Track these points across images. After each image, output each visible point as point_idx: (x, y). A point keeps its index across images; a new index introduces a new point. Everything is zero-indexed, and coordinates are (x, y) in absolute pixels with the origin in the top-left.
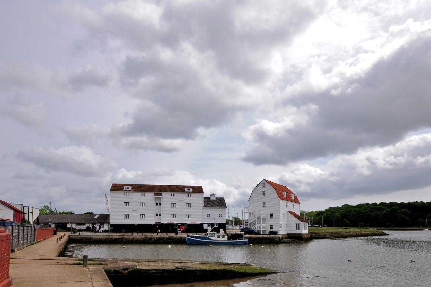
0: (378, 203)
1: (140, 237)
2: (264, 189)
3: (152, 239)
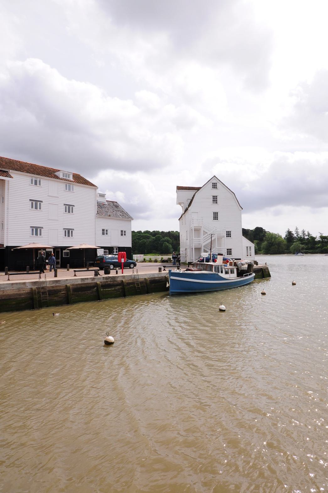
0: (143, 232)
1: (19, 289)
2: (215, 192)
3: (60, 291)
